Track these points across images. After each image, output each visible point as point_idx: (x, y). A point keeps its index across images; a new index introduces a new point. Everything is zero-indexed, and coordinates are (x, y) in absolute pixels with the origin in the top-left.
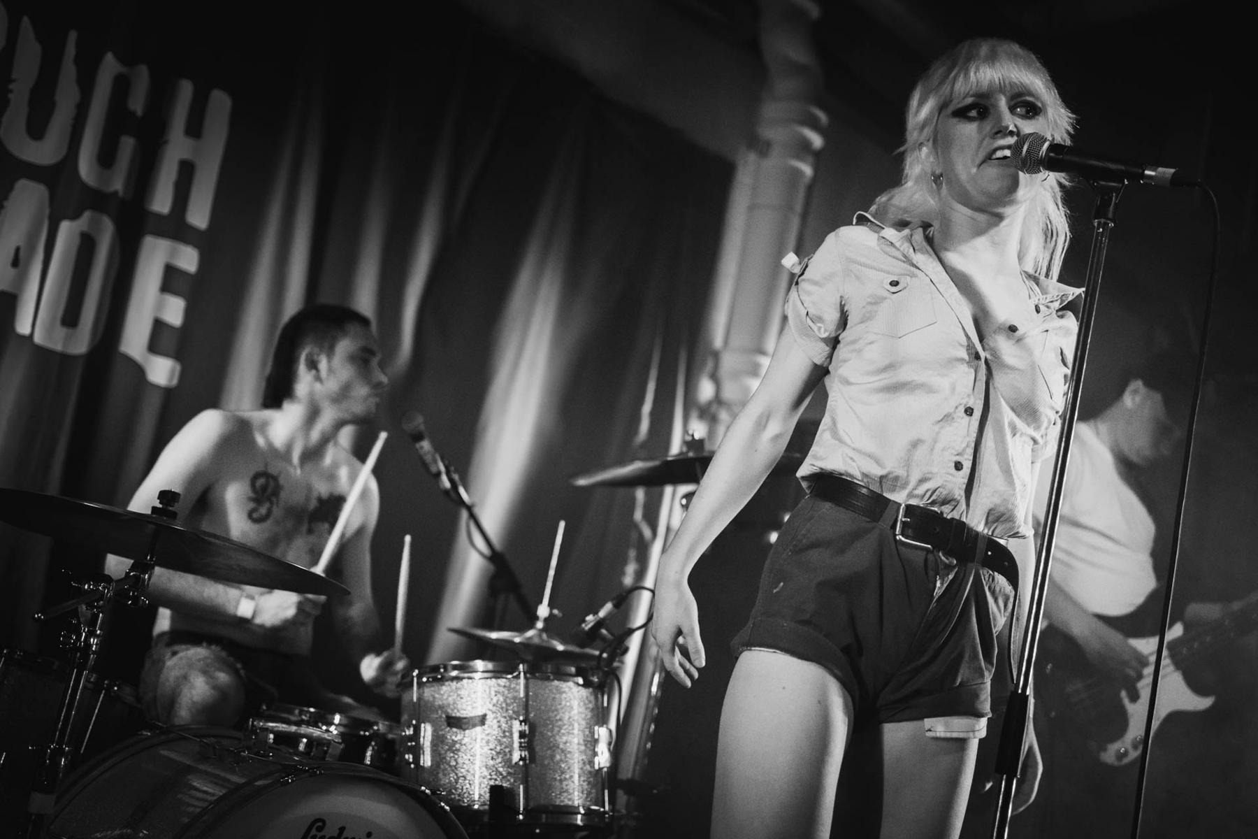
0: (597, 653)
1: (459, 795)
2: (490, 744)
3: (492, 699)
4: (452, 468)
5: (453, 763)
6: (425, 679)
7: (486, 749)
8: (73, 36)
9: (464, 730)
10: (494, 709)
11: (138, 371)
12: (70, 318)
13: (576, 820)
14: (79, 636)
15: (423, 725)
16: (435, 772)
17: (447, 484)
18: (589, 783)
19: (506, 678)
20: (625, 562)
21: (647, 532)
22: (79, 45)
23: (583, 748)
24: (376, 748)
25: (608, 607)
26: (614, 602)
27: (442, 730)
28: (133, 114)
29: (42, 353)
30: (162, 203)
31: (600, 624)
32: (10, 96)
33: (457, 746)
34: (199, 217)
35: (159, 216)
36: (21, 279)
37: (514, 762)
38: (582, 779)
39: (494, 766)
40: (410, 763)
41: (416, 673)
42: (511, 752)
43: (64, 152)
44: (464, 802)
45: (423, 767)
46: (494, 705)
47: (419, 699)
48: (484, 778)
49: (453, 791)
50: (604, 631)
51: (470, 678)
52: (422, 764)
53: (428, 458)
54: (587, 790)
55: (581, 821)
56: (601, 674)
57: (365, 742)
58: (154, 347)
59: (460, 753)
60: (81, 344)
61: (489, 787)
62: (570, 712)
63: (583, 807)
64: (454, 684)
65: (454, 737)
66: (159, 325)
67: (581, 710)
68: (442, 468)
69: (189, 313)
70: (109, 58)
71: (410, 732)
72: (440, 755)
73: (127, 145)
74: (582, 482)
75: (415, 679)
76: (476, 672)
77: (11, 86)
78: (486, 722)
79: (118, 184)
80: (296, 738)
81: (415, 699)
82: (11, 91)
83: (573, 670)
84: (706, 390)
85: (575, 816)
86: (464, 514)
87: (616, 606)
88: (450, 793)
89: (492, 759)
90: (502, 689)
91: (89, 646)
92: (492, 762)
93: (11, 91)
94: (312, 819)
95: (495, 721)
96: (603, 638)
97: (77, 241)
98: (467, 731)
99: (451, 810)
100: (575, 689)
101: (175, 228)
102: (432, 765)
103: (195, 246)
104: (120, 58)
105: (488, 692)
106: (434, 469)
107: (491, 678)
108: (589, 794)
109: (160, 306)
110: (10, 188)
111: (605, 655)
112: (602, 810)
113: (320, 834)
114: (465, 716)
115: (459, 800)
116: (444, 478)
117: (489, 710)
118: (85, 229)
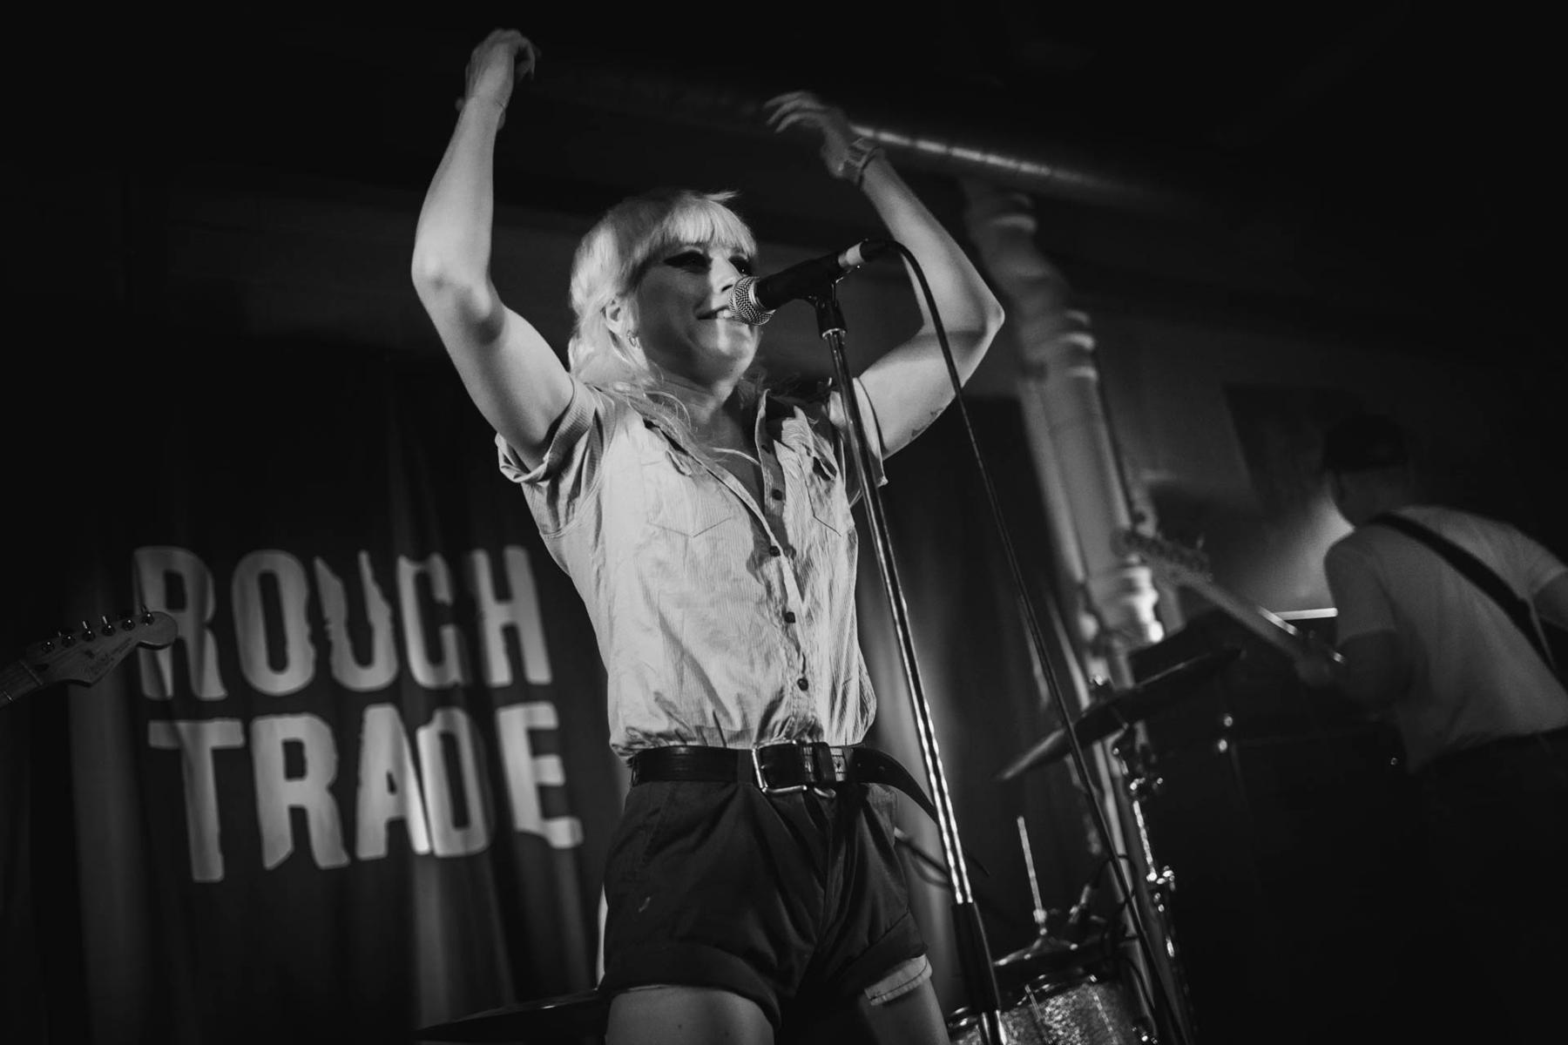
8: (364, 558)
11: (541, 841)
12: (460, 818)
20: (1084, 833)
22: (374, 563)
28: (442, 605)
29: (448, 865)
30: (500, 673)
34: (539, 671)
36: (402, 803)
43: (394, 666)
58: (547, 813)
60: (478, 837)
69: (567, 768)
73: (449, 634)
74: (1009, 774)
79: (454, 673)
84: (1089, 626)
86: (906, 853)
97: (437, 744)
101: (522, 692)
109: (537, 771)
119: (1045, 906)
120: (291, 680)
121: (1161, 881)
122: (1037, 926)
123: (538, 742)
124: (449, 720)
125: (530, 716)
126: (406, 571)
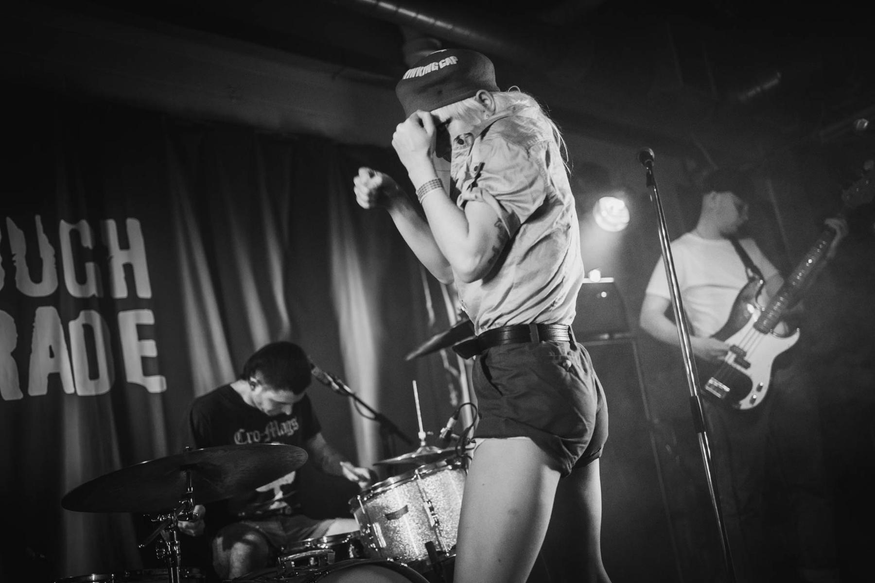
0: (453, 449)
4: (336, 377)
5: (399, 539)
7: (414, 525)
8: (38, 218)
9: (398, 518)
10: (410, 501)
11: (143, 389)
12: (94, 374)
14: (167, 548)
15: (374, 525)
16: (390, 549)
17: (337, 387)
19: (410, 481)
21: (454, 372)
25: (451, 421)
26: (453, 417)
27: (385, 524)
28: (88, 248)
30: (121, 291)
31: (449, 433)
32: (15, 264)
33: (398, 529)
34: (144, 291)
35: (122, 300)
36: (58, 363)
37: (432, 525)
39: (422, 532)
41: (359, 497)
43: (56, 284)
45: (383, 548)
46: (410, 499)
47: (366, 510)
48: (419, 541)
49: (405, 555)
50: (453, 435)
51: (390, 489)
52: (381, 546)
56: (460, 459)
57: (347, 546)
59: (401, 532)
60: (104, 385)
61: (424, 545)
65: (394, 525)
66: (144, 360)
67: (457, 483)
68: (330, 379)
69: (159, 347)
70: (63, 222)
71: (368, 531)
72: (390, 537)
73: (90, 267)
74: (410, 357)
75: (360, 501)
77: (14, 259)
79: (92, 290)
81: (364, 512)
82: (15, 261)
83: (444, 463)
86: (352, 400)
87: (456, 418)
88: (404, 557)
89: (420, 528)
91: (174, 552)
93: (15, 261)
95: (413, 507)
96: (455, 439)
97: (82, 331)
98: (400, 519)
101: (133, 302)
102: (387, 545)
103: (149, 308)
104: (70, 221)
105: (403, 492)
106: (326, 382)
107: (402, 484)
109: (141, 349)
110: (34, 315)
111: (459, 448)
114: (395, 511)
115: (410, 559)
116: (334, 384)
117: (408, 502)
118: (84, 322)
119: (425, 430)
122: (420, 440)
123: (142, 332)
125: (138, 317)
126: (65, 228)
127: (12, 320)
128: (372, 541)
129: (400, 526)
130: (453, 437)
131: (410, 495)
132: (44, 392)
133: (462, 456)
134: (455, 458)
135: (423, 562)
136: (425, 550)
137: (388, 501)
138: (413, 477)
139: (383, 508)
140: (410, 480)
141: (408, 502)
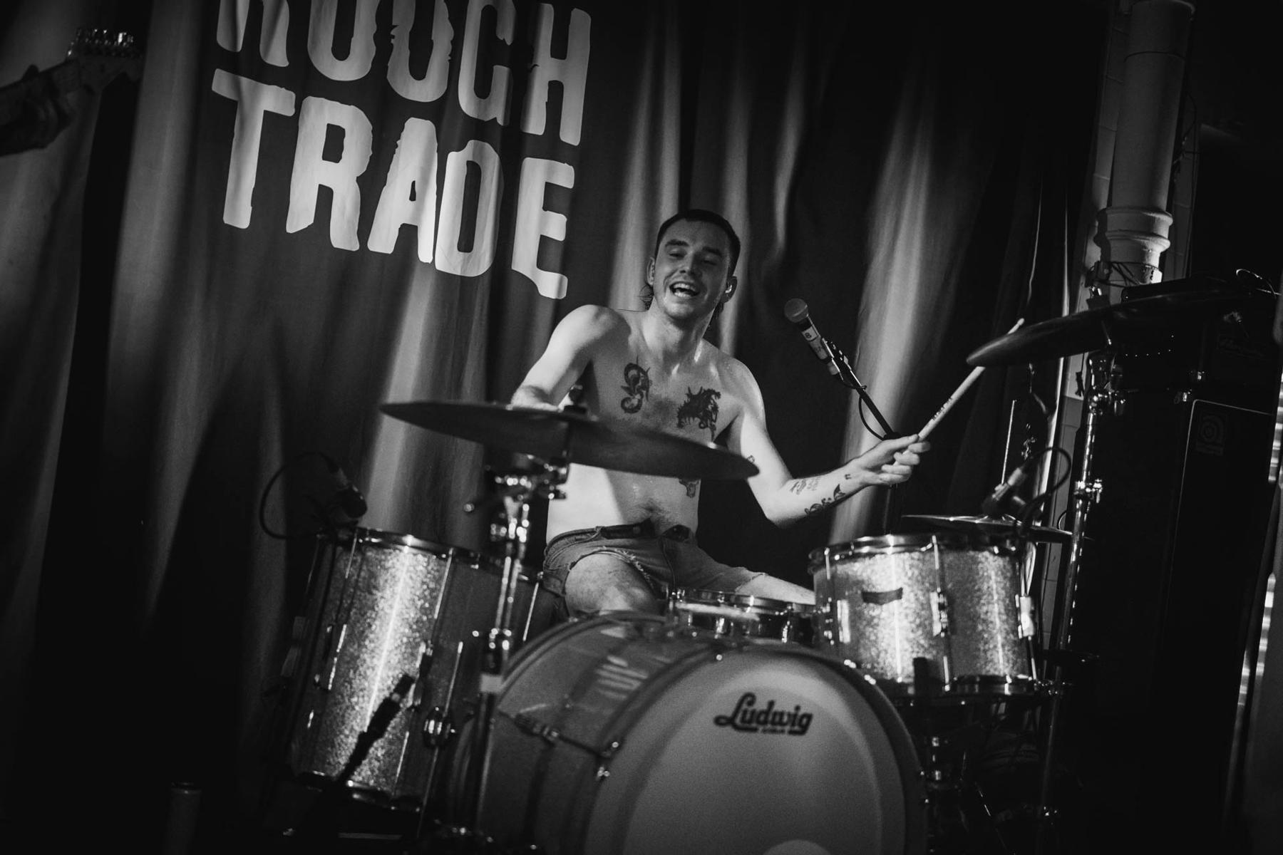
1: (882, 669)
2: (909, 617)
3: (907, 573)
5: (873, 638)
6: (837, 557)
7: (905, 623)
9: (881, 604)
11: (531, 286)
12: (466, 243)
13: (1004, 689)
15: (839, 602)
18: (1014, 652)
23: (1004, 617)
24: (791, 627)
26: (1022, 467)
27: (859, 606)
29: (445, 278)
30: (536, 125)
31: (1010, 492)
32: (393, 41)
33: (876, 621)
34: (571, 134)
36: (419, 212)
37: (935, 634)
38: (1006, 648)
39: (914, 639)
40: (829, 640)
41: (827, 552)
42: (931, 625)
44: (887, 675)
45: (842, 643)
49: (876, 665)
50: (1017, 499)
51: (882, 553)
53: (816, 344)
54: (1013, 659)
55: (1010, 689)
57: (781, 621)
58: (542, 264)
61: (912, 660)
62: (988, 582)
63: (1011, 676)
64: (867, 561)
65: (871, 612)
66: (544, 240)
67: (999, 579)
71: (827, 609)
72: (858, 630)
73: (501, 75)
76: (888, 546)
77: (393, 33)
78: (903, 596)
79: (497, 112)
80: (715, 618)
81: (829, 577)
82: (393, 37)
85: (1002, 686)
86: (856, 395)
88: (873, 667)
90: (916, 562)
92: (912, 636)
93: (393, 37)
94: (741, 695)
95: (912, 595)
96: (1017, 505)
98: (884, 606)
99: (877, 683)
100: (991, 558)
102: (852, 641)
107: (904, 552)
108: (1015, 663)
109: (543, 223)
110: (402, 128)
112: (1030, 679)
113: (750, 709)
115: (882, 674)
117: (905, 583)
118: (471, 159)
120: (347, 71)
121: (1088, 490)
124: (479, 152)
125: (550, 171)
127: (372, 128)
128: (828, 627)
129: (881, 617)
130: (1015, 501)
131: (913, 574)
132: (389, 249)
133: (1023, 537)
134: (1007, 537)
135: (903, 686)
136: (911, 669)
137: (873, 571)
138: (926, 545)
139: (863, 582)
140: (918, 549)
141: (905, 583)
